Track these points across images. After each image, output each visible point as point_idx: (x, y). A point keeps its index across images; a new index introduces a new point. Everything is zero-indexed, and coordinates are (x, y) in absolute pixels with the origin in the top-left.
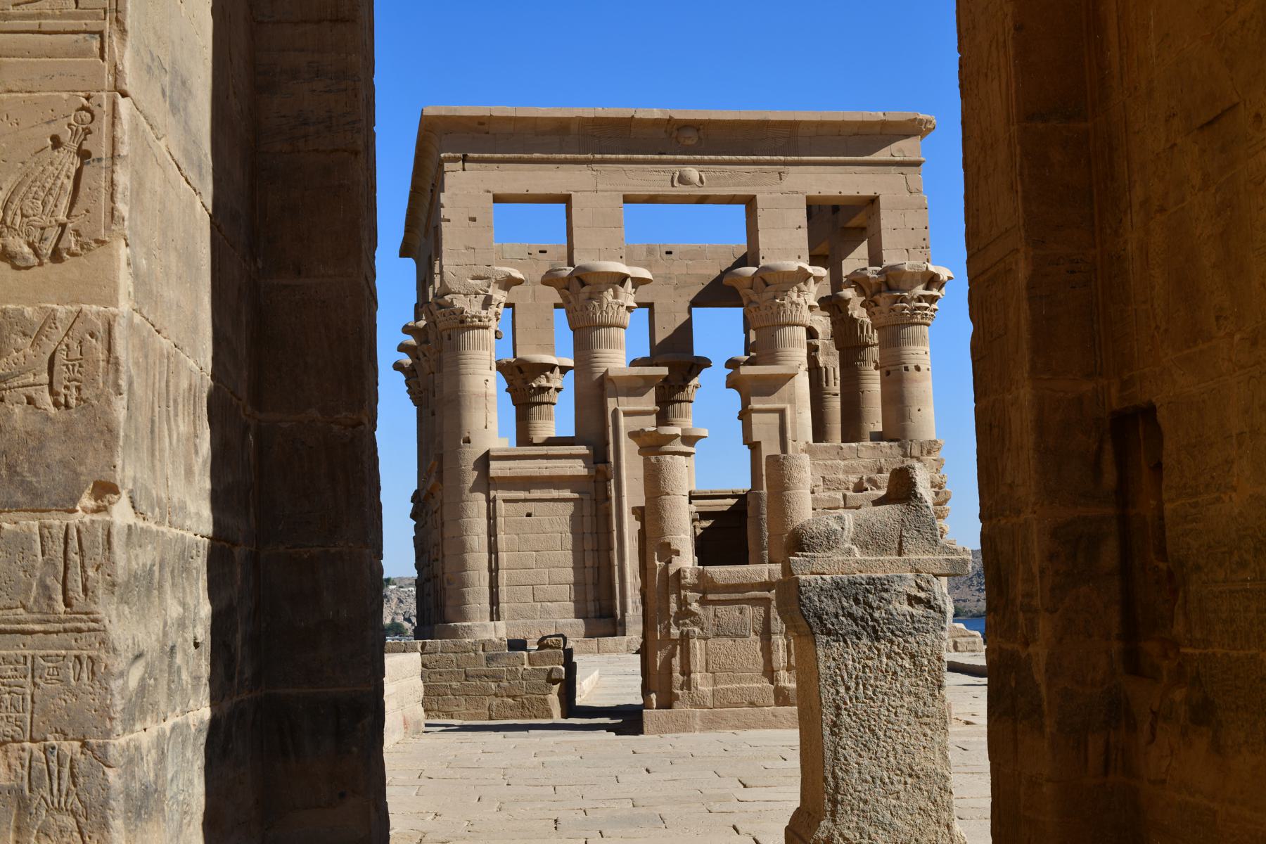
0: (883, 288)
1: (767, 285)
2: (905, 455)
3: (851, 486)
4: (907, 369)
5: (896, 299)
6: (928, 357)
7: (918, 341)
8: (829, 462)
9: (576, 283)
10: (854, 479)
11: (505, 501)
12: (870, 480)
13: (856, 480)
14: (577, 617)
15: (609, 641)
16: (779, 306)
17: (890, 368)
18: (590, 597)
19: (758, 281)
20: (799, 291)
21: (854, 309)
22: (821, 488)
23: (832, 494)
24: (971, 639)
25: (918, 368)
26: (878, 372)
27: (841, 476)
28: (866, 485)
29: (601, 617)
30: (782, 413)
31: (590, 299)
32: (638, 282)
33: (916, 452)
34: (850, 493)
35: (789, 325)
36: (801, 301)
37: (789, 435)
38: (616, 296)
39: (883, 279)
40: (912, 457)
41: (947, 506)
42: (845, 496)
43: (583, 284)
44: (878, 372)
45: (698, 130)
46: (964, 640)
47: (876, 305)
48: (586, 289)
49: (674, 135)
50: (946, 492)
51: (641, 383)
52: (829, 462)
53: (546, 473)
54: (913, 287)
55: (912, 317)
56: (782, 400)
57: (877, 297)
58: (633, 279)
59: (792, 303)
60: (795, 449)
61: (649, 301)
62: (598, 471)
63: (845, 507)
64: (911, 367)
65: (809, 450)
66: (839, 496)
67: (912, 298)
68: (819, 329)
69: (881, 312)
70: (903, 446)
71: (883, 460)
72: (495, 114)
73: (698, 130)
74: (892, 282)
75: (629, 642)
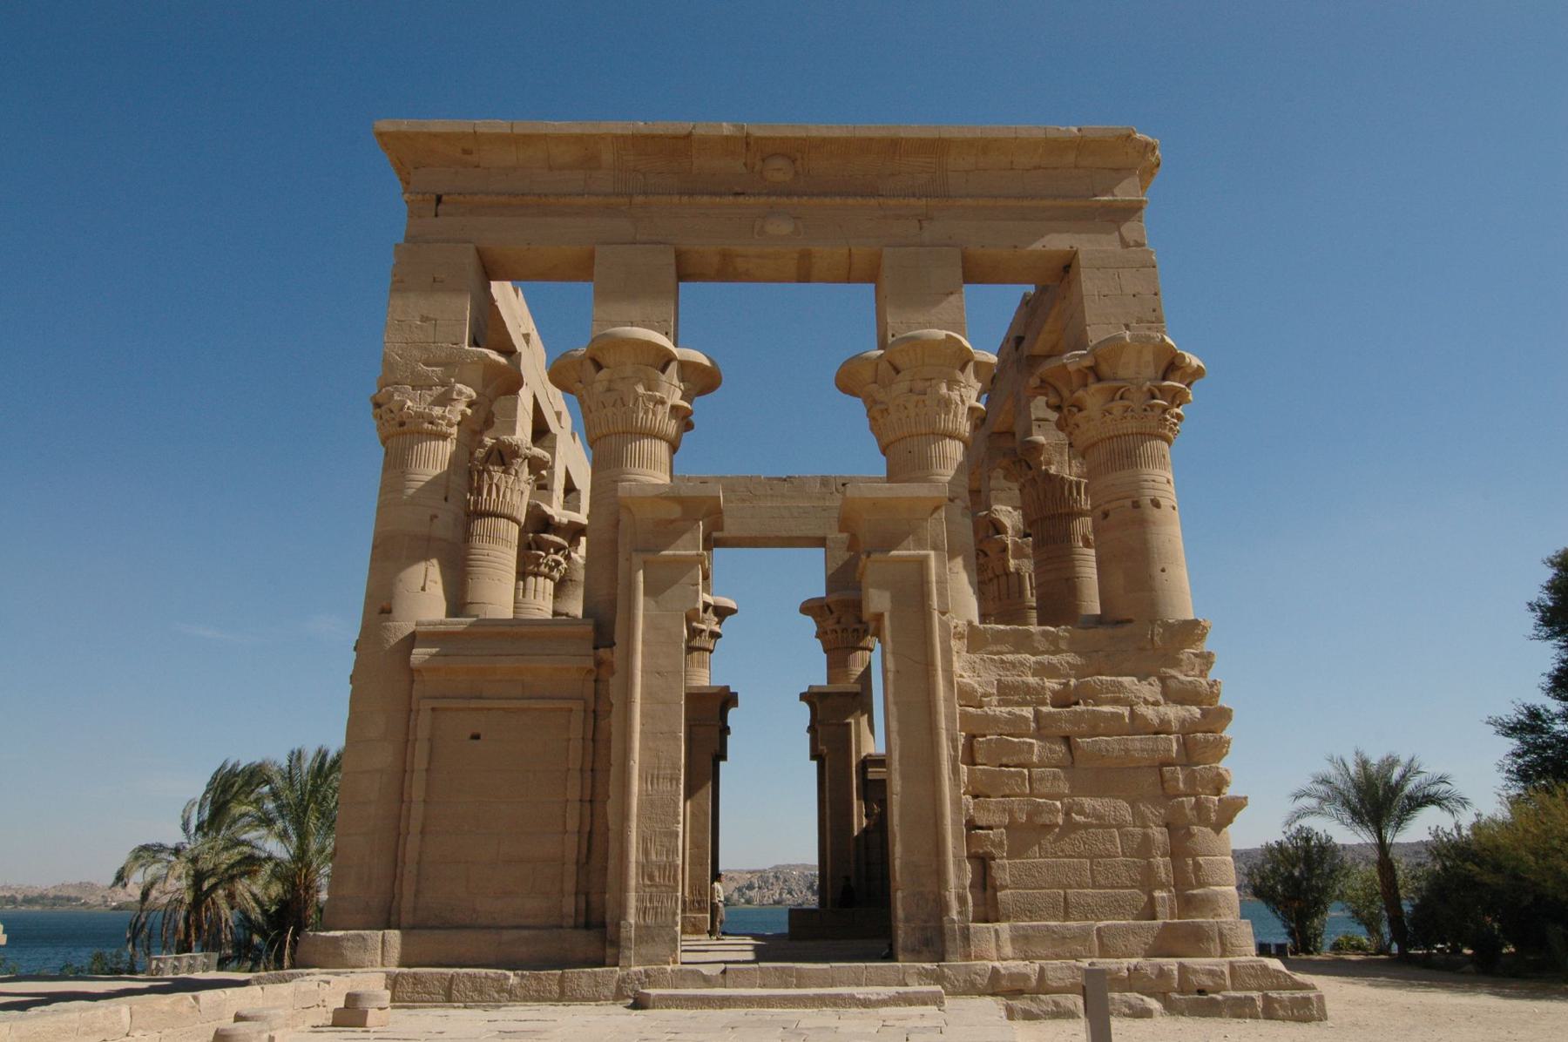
0: (1091, 379)
1: (898, 372)
6: (1171, 488)
7: (1158, 461)
8: (1010, 657)
9: (590, 367)
10: (1052, 684)
15: (582, 977)
17: (1107, 507)
18: (570, 886)
19: (884, 366)
22: (995, 700)
23: (1016, 710)
24: (1299, 994)
25: (1157, 504)
26: (1092, 552)
27: (1031, 680)
29: (587, 926)
32: (702, 381)
36: (955, 395)
39: (1088, 362)
41: (1226, 734)
42: (1037, 714)
43: (599, 367)
44: (1092, 552)
45: (794, 161)
46: (1286, 994)
47: (1080, 410)
48: (603, 374)
49: (757, 168)
51: (676, 511)
52: (1010, 657)
56: (920, 544)
57: (1080, 393)
58: (684, 365)
60: (945, 626)
61: (820, 533)
62: (599, 663)
63: (1038, 734)
64: (1146, 501)
65: (975, 640)
68: (1007, 522)
72: (480, 130)
73: (794, 161)
74: (1104, 369)
75: (623, 980)
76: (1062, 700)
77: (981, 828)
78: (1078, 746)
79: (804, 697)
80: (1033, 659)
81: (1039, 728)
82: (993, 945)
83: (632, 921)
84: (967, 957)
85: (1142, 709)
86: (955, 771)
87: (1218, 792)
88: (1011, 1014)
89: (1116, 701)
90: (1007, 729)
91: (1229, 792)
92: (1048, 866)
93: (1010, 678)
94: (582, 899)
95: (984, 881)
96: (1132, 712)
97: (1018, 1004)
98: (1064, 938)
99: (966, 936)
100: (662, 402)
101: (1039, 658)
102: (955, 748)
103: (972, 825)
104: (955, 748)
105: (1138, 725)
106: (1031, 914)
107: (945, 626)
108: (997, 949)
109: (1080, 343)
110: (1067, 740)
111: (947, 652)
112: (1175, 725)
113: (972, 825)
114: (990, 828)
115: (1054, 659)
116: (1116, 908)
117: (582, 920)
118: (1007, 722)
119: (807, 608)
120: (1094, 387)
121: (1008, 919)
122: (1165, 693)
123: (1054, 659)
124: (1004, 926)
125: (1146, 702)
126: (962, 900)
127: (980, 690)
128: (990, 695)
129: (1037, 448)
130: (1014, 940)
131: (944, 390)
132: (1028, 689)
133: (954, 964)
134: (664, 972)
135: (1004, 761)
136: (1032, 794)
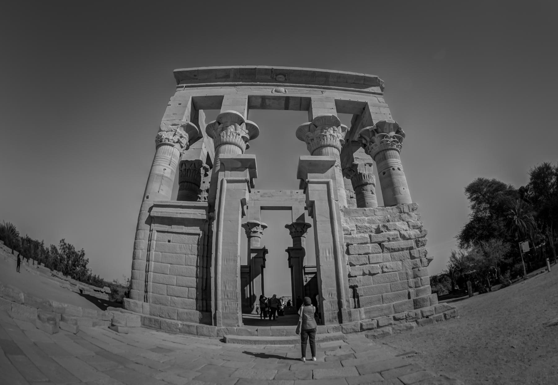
1: (316, 127)
2: (401, 212)
3: (374, 231)
4: (394, 169)
5: (383, 136)
8: (359, 218)
10: (374, 226)
11: (157, 231)
12: (384, 226)
13: (375, 227)
14: (197, 310)
16: (324, 136)
17: (385, 171)
19: (312, 126)
20: (334, 130)
21: (360, 170)
22: (355, 232)
23: (363, 235)
28: (382, 229)
30: (328, 183)
31: (222, 130)
33: (406, 210)
34: (372, 234)
35: (329, 146)
37: (333, 196)
38: (236, 130)
40: (404, 213)
41: (426, 238)
42: (370, 236)
50: (425, 231)
52: (359, 218)
53: (179, 216)
54: (390, 132)
55: (392, 146)
57: (373, 138)
59: (331, 135)
60: (337, 205)
63: (371, 243)
64: (396, 168)
65: (346, 212)
66: (367, 235)
67: (391, 137)
69: (376, 145)
70: (398, 208)
71: (389, 216)
75: (218, 330)
76: (378, 231)
77: (352, 277)
78: (383, 245)
79: (286, 251)
80: (366, 218)
81: (371, 240)
82: (359, 315)
83: (221, 311)
84: (350, 321)
85: (403, 232)
86: (344, 256)
87: (425, 256)
88: (367, 336)
89: (395, 230)
90: (360, 242)
91: (428, 256)
92: (376, 287)
93: (359, 224)
94: (205, 302)
95: (355, 295)
96: (400, 234)
97: (370, 333)
98: (382, 310)
99: (350, 314)
100: (239, 135)
101: (368, 218)
102: (343, 248)
103: (350, 276)
104: (343, 248)
105: (404, 237)
106: (371, 303)
107: (337, 205)
108: (361, 316)
109: (371, 124)
110: (380, 244)
111: (338, 214)
112: (413, 237)
113: (350, 276)
114: (356, 276)
115: (374, 218)
116: (398, 297)
117: (205, 309)
118: (360, 239)
119: (287, 226)
120: (377, 135)
121: (363, 306)
122: (409, 226)
123: (374, 218)
124: (362, 309)
125: (403, 230)
126: (348, 301)
127: (350, 229)
128: (353, 230)
129: (356, 165)
130: (365, 313)
131: (332, 132)
132: (367, 228)
133: (346, 324)
134: (234, 329)
135: (360, 253)
136: (370, 264)
